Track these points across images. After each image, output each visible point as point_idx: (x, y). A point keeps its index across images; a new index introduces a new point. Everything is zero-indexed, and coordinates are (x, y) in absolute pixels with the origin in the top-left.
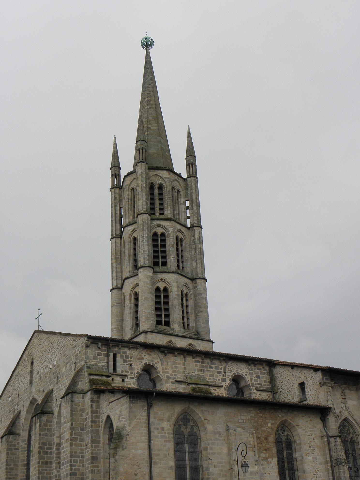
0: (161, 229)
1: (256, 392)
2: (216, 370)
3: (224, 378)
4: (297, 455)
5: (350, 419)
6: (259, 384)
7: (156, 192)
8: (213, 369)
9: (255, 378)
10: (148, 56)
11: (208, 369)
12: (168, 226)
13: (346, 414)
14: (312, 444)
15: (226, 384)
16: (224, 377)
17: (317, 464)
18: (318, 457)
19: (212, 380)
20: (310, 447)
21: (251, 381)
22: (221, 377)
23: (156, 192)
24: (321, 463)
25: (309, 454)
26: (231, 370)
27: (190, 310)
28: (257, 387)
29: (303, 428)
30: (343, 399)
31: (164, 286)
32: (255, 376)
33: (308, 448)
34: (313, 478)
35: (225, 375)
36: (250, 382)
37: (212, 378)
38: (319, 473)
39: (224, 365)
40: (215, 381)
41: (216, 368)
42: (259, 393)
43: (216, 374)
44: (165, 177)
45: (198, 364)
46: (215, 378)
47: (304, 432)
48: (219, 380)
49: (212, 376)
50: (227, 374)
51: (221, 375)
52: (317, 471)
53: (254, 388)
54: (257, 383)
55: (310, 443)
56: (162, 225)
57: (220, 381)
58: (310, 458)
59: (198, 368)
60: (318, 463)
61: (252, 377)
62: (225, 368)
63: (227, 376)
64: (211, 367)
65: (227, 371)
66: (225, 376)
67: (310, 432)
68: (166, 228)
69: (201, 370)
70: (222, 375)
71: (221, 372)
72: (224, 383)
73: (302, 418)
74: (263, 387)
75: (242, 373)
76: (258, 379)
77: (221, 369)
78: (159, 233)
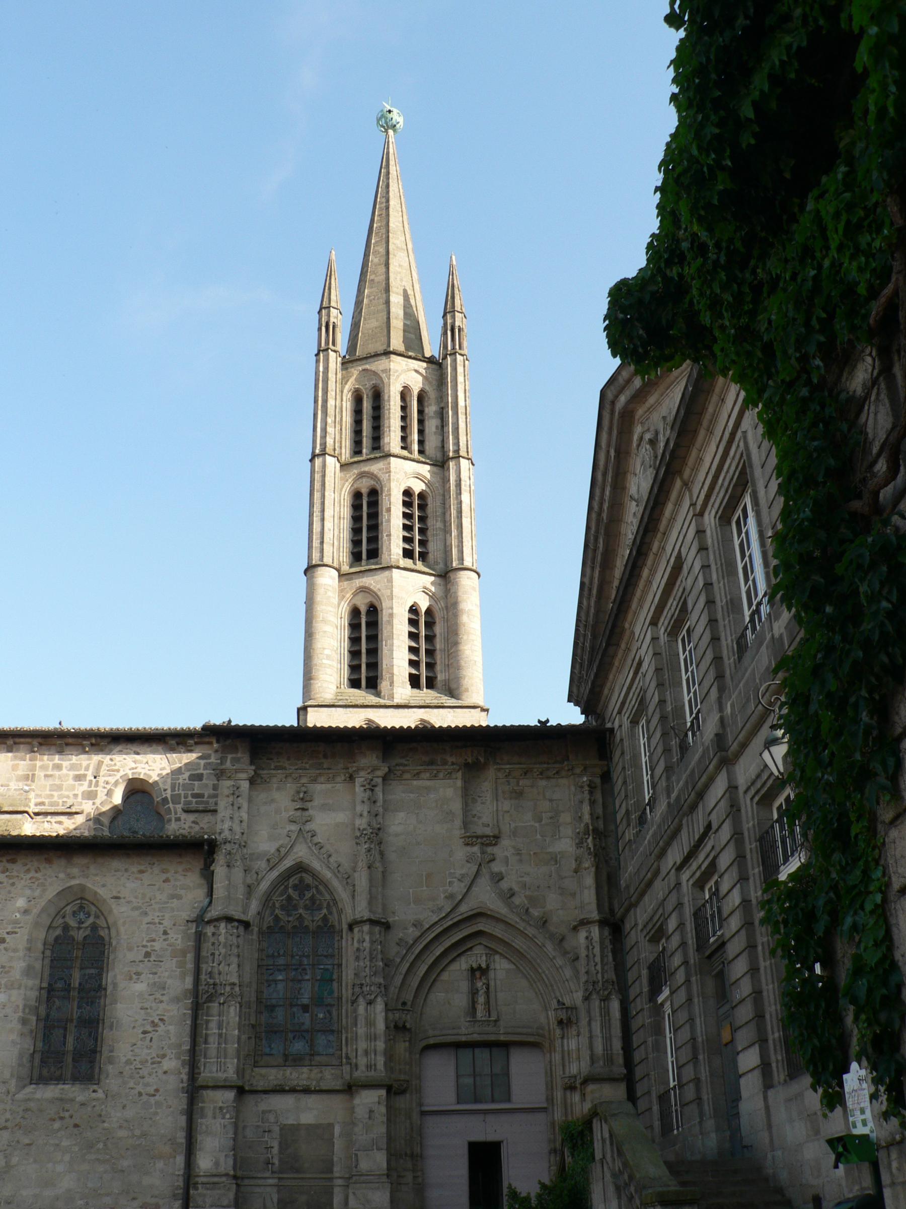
0: (369, 480)
1: (184, 816)
2: (72, 773)
3: (92, 791)
4: (109, 978)
5: (316, 865)
6: (195, 796)
7: (367, 405)
8: (64, 771)
9: (187, 781)
10: (387, 143)
11: (50, 773)
12: (380, 470)
13: (301, 853)
14: (157, 945)
15: (94, 804)
16: (93, 788)
17: (161, 1002)
18: (169, 981)
19: (55, 799)
20: (147, 955)
21: (173, 789)
22: (85, 787)
23: (367, 405)
24: (176, 1000)
25: (138, 974)
26: (116, 768)
27: (439, 644)
28: (190, 803)
29: (135, 904)
30: (296, 810)
31: (367, 601)
32: (186, 775)
33: (141, 958)
34: (139, 1043)
35: (97, 782)
36: (168, 794)
37: (55, 794)
38: (162, 1028)
39: (96, 758)
40: (65, 800)
41: (72, 767)
42: (192, 817)
43: (71, 782)
44: (382, 371)
45: (22, 762)
46: (66, 793)
47: (137, 913)
48: (76, 796)
49: (59, 788)
50: (101, 780)
51: (82, 785)
52: (156, 1021)
53: (179, 807)
54: (190, 793)
55: (149, 944)
56: (368, 473)
57: (80, 799)
58: (140, 987)
59: (20, 772)
60: (164, 998)
61: (178, 779)
62: (100, 763)
63: (101, 784)
64: (58, 767)
65: (101, 774)
66: (97, 785)
67: (157, 914)
68: (376, 476)
69: (26, 778)
70: (86, 784)
71: (85, 776)
72: (91, 802)
73: (139, 876)
74: (207, 803)
75: (148, 772)
76: (196, 783)
77: (87, 769)
78: (364, 491)
